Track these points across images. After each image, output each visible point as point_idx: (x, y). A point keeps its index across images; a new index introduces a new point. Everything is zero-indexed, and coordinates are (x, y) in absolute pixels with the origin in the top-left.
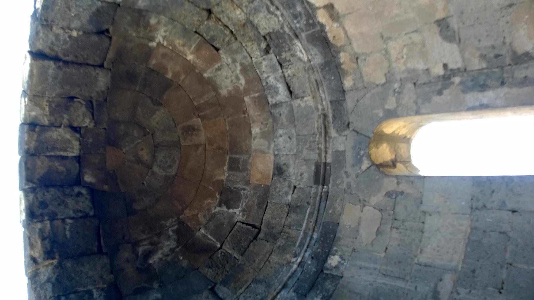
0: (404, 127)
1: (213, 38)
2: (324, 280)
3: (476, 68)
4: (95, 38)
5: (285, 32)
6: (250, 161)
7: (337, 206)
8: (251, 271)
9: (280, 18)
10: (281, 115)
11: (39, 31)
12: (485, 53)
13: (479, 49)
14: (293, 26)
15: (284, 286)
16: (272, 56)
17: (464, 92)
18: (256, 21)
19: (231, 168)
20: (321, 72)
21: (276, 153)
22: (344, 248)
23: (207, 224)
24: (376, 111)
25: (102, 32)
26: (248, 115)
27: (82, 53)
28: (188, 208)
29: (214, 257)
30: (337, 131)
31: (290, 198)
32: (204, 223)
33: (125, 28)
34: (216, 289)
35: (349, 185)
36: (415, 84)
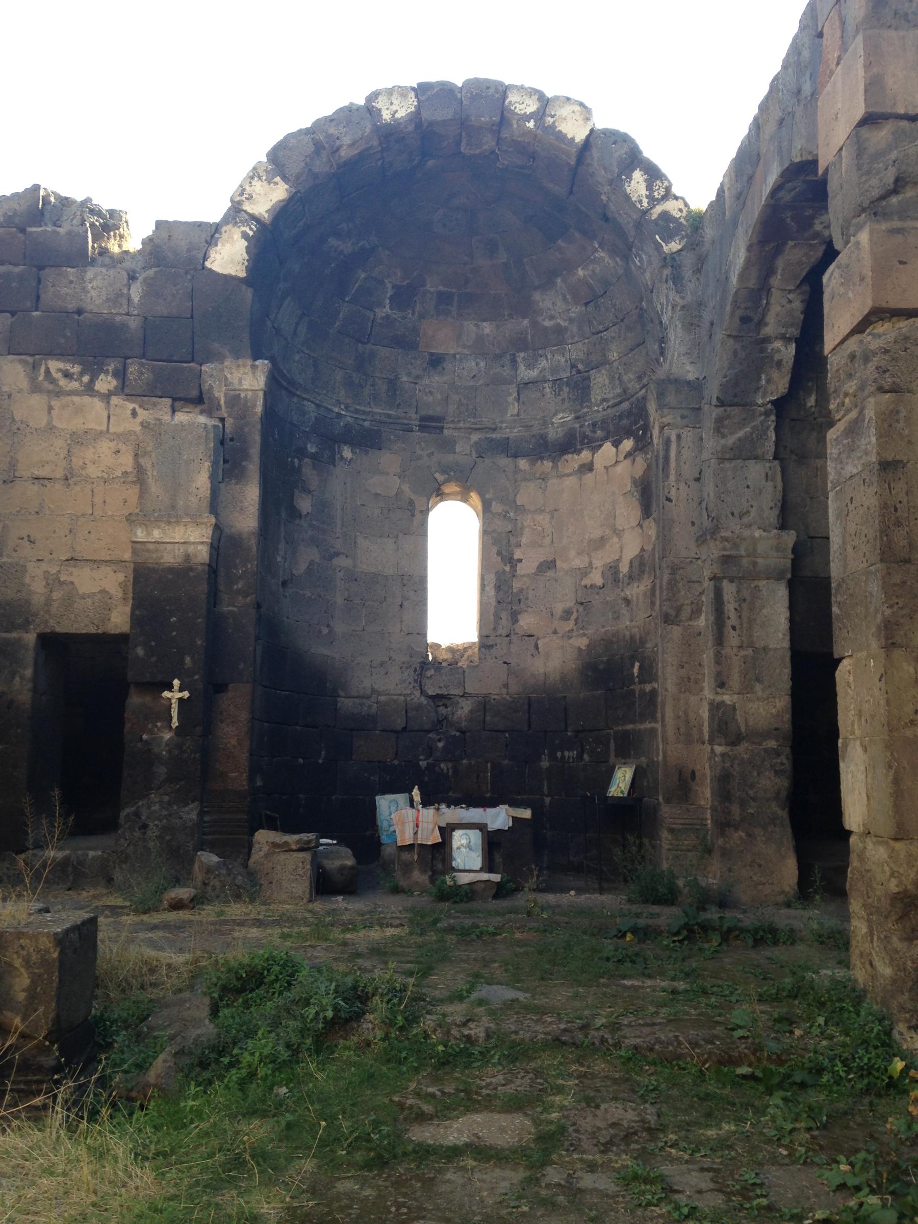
5: (582, 407)
10: (503, 366)
15: (318, 406)
17: (497, 573)
18: (603, 371)
19: (440, 294)
21: (458, 356)
30: (476, 443)
31: (405, 379)
35: (419, 458)
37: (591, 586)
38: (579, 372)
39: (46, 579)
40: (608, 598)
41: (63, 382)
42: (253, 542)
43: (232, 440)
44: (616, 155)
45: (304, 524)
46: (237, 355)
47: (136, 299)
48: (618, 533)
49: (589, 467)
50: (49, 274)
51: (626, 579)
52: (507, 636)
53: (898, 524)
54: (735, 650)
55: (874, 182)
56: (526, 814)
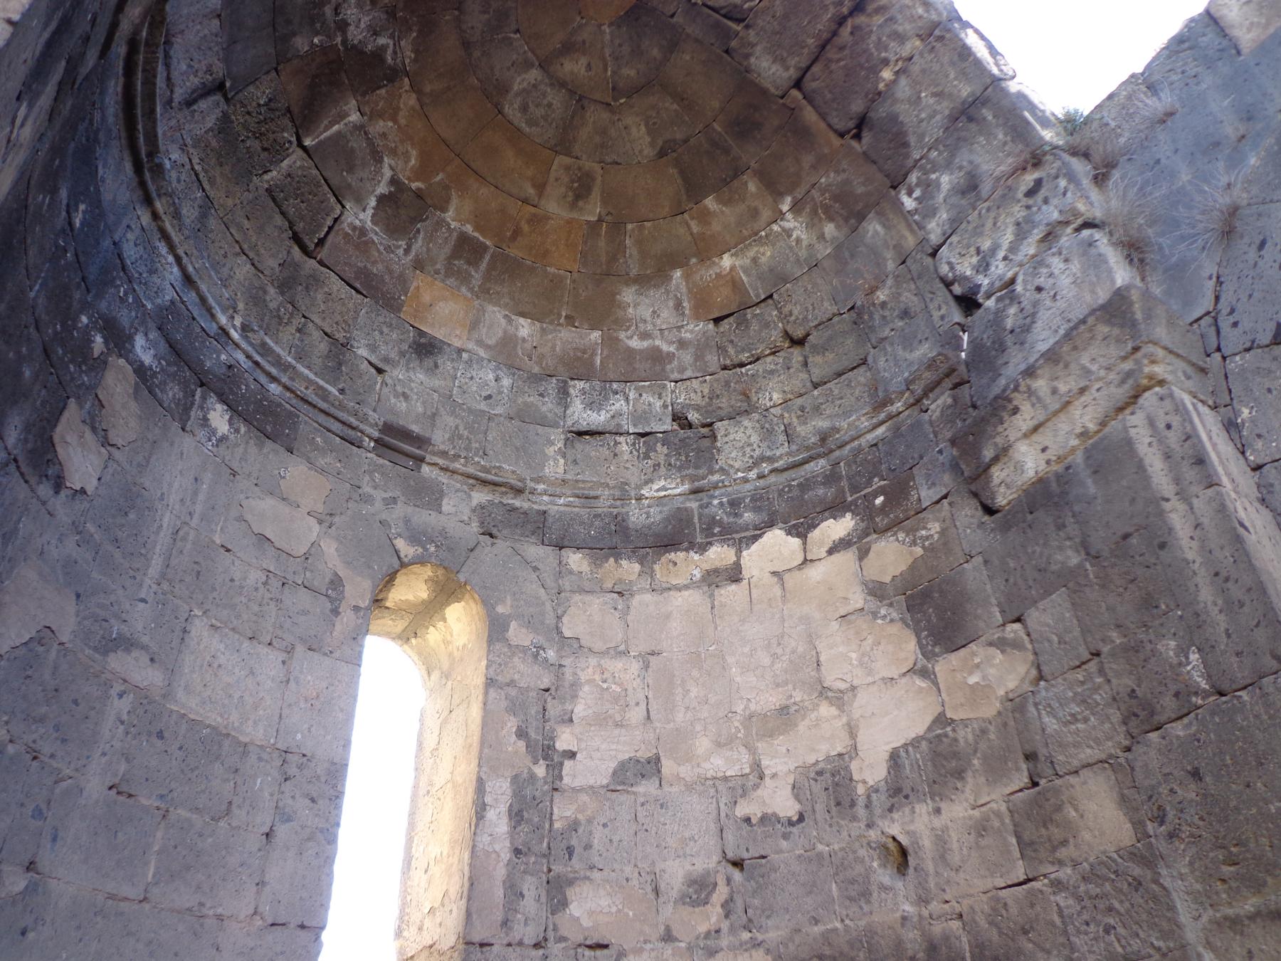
0: (446, 643)
1: (743, 323)
2: (185, 385)
3: (556, 810)
4: (857, 107)
5: (712, 472)
6: (464, 289)
7: (328, 460)
8: (230, 202)
9: (740, 475)
10: (541, 395)
11: (927, 11)
12: (580, 831)
13: (590, 821)
14: (717, 493)
15: (188, 280)
16: (668, 425)
17: (515, 779)
18: (746, 423)
19: (463, 239)
20: (611, 513)
21: (465, 355)
22: (241, 449)
23: (366, 133)
24: (509, 602)
25: (861, 125)
26: (559, 325)
27: (842, 63)
28: (418, 107)
29: (286, 121)
31: (362, 352)
32: (371, 129)
33: (844, 171)
34: (218, 97)
35: (367, 499)
36: (547, 690)
37: (764, 819)
40: (820, 847)
49: (734, 574)
51: (879, 800)
52: (537, 946)
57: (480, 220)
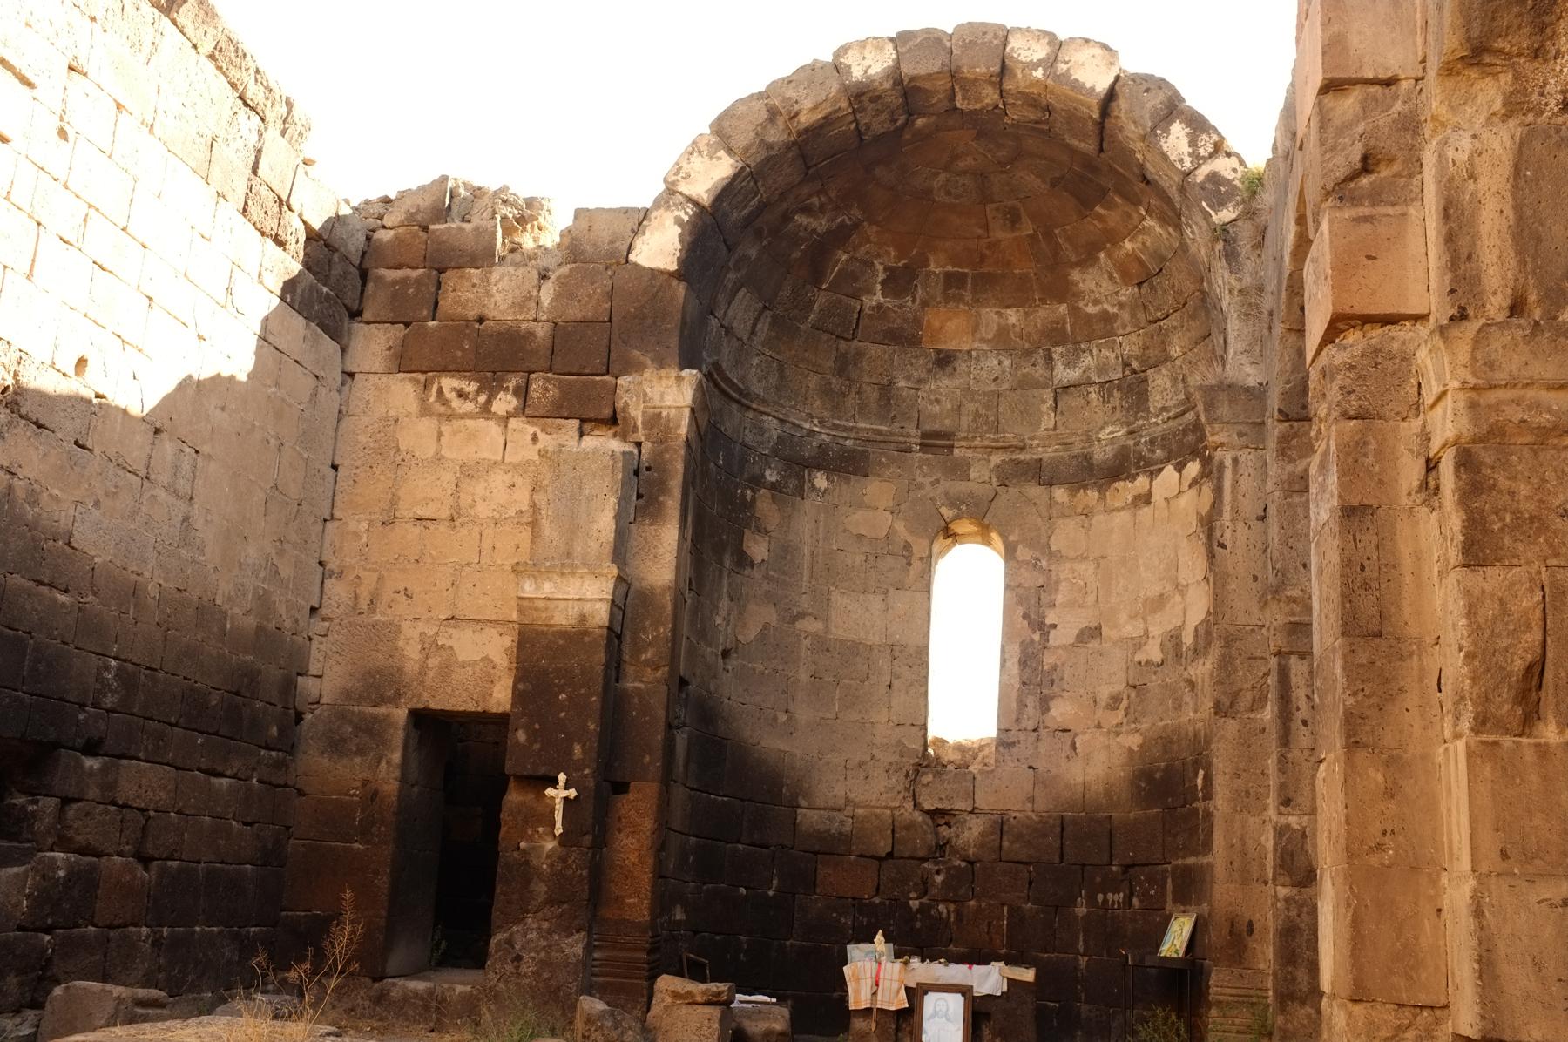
1: (1152, 288)
15: (782, 421)
19: (948, 275)
30: (998, 466)
31: (902, 383)
35: (920, 486)
37: (1148, 663)
38: (1134, 372)
39: (422, 642)
41: (456, 403)
42: (668, 601)
43: (648, 469)
44: (1148, 105)
45: (756, 574)
46: (661, 364)
47: (546, 301)
48: (1180, 589)
49: (1145, 499)
50: (450, 278)
53: (1366, 586)
54: (1306, 753)
55: (1340, 159)
56: (1028, 975)
57: (954, 260)
